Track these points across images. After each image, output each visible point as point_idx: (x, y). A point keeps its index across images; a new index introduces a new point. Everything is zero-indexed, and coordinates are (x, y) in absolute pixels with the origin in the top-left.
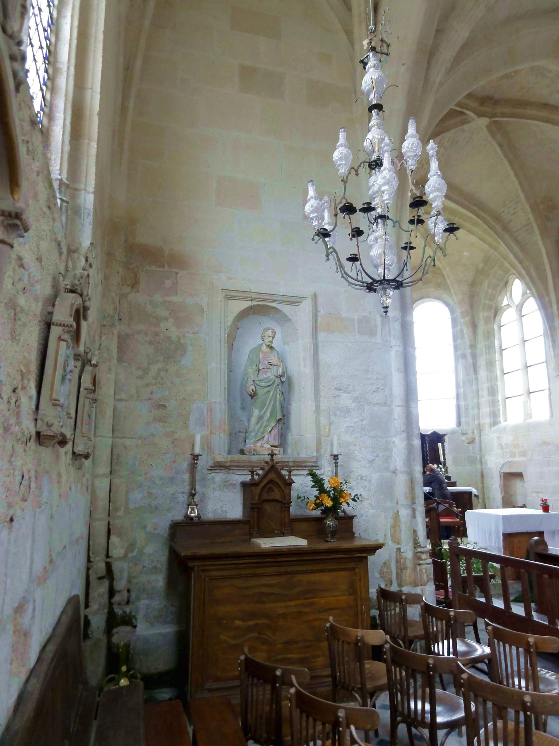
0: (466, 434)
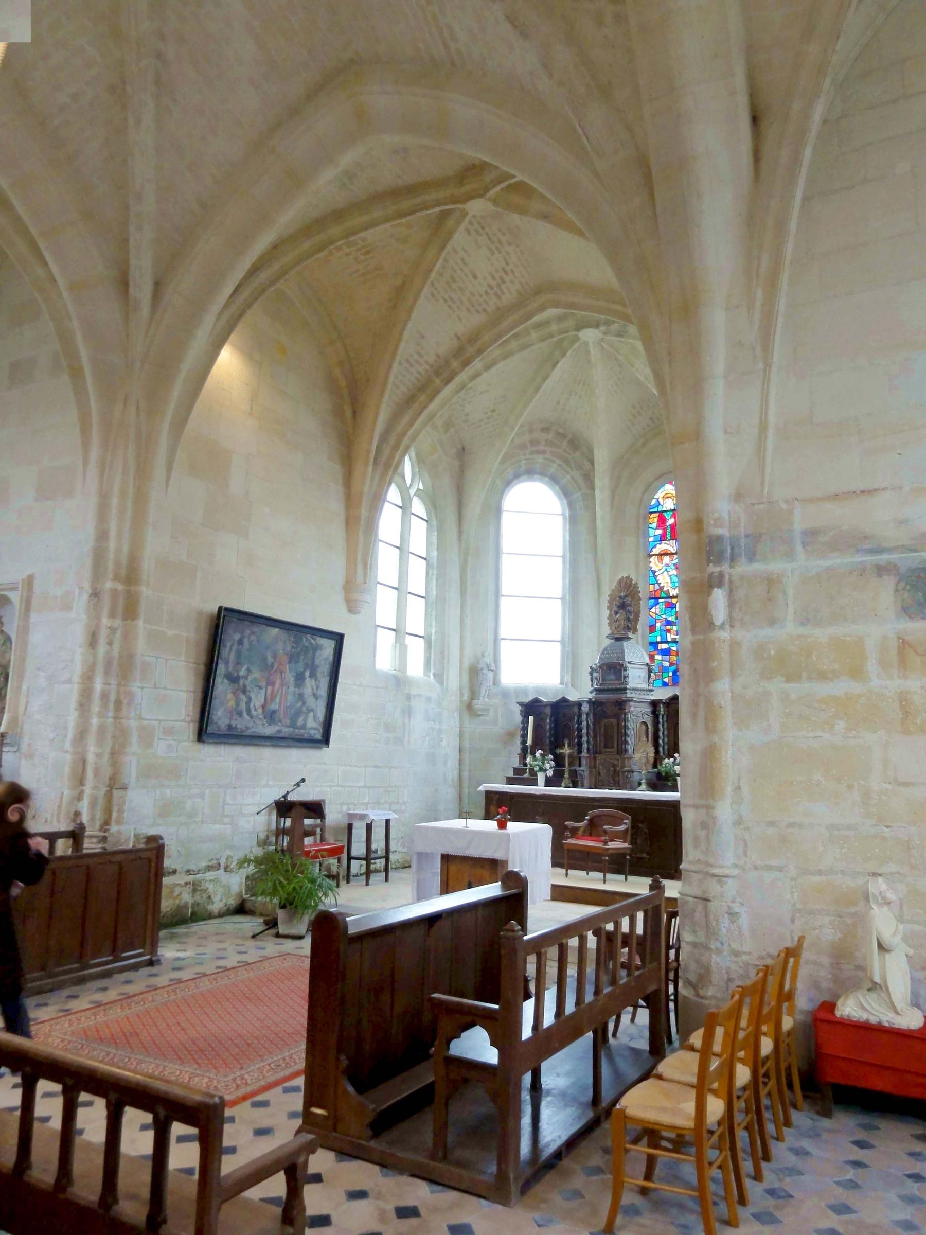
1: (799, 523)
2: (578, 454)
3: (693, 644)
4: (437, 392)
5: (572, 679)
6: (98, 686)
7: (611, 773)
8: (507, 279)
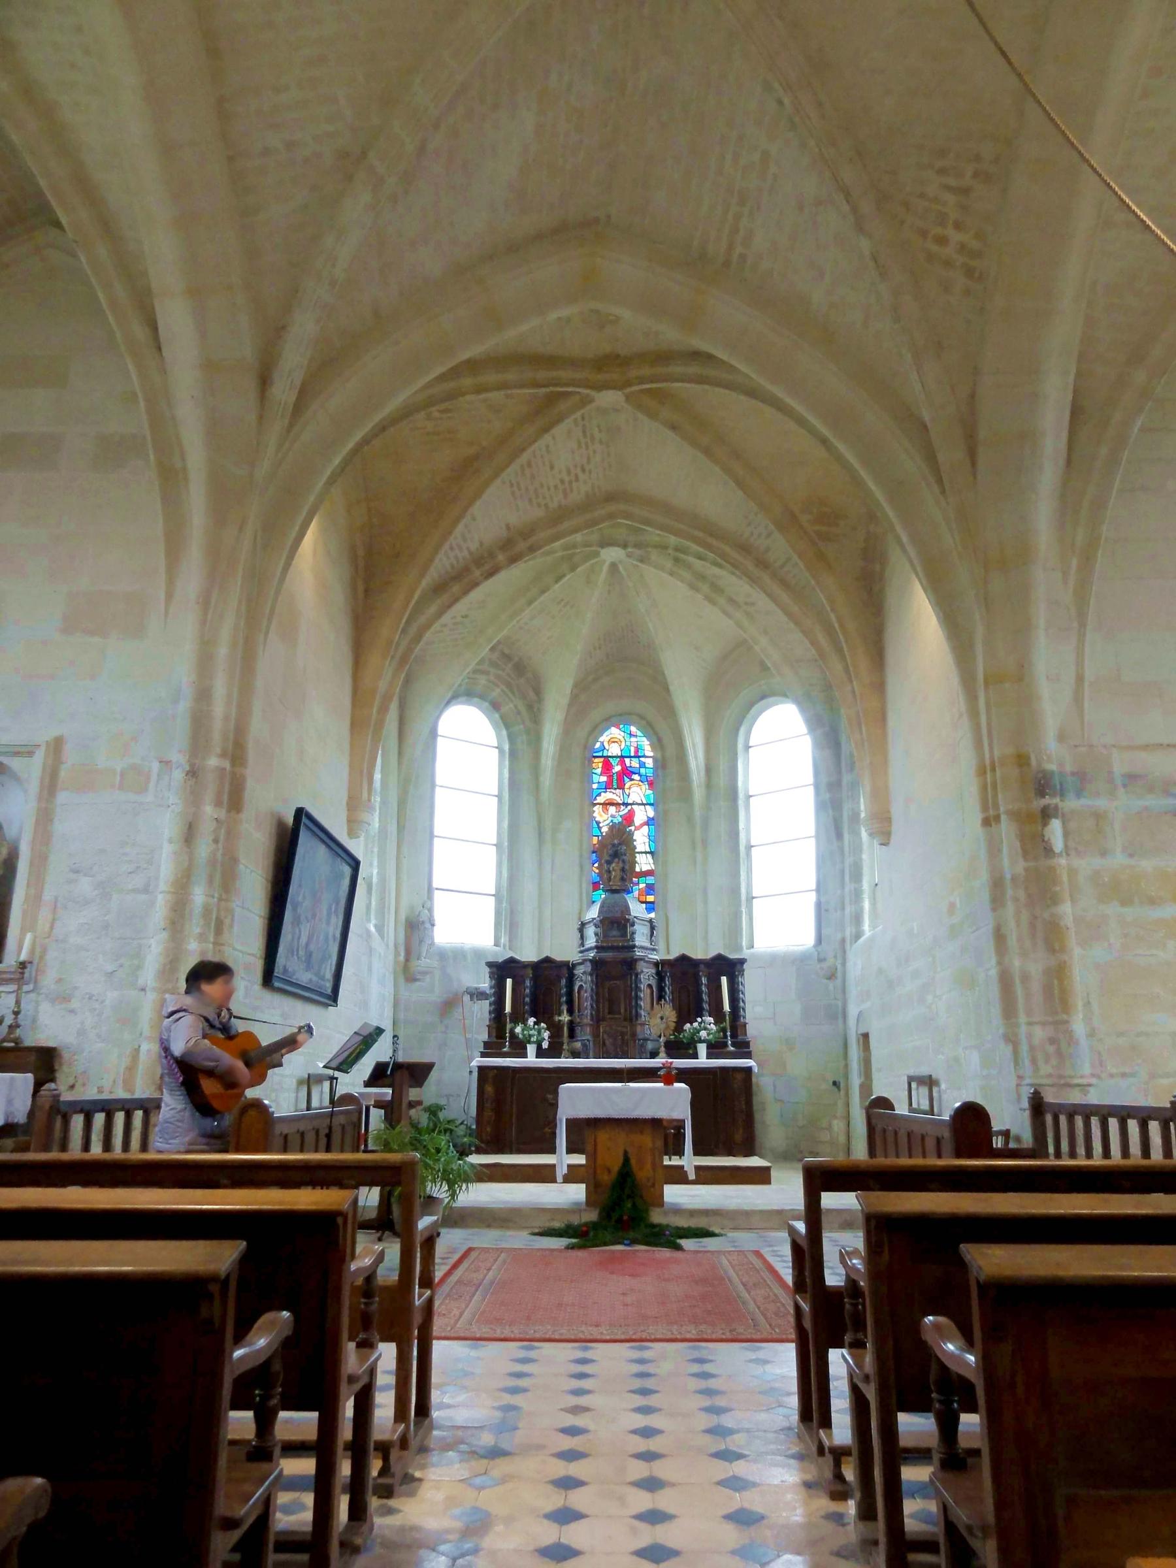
0: (825, 960)
1: (1120, 765)
2: (522, 681)
3: (1026, 870)
4: (476, 584)
5: (510, 941)
6: (199, 896)
7: (619, 1042)
8: (581, 476)
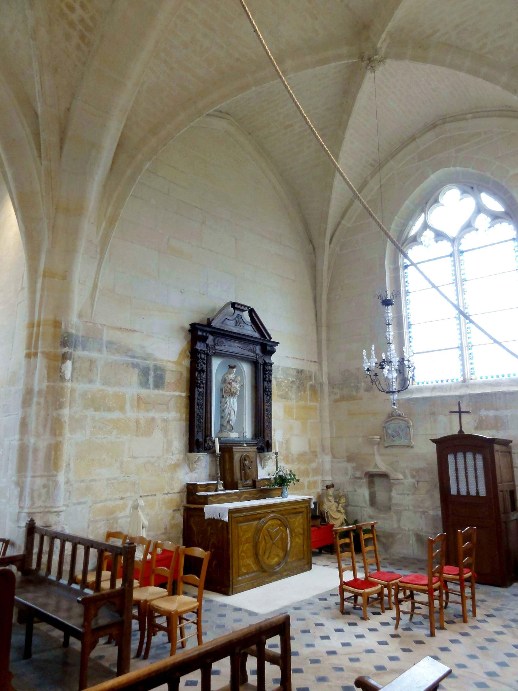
3: (47, 387)
